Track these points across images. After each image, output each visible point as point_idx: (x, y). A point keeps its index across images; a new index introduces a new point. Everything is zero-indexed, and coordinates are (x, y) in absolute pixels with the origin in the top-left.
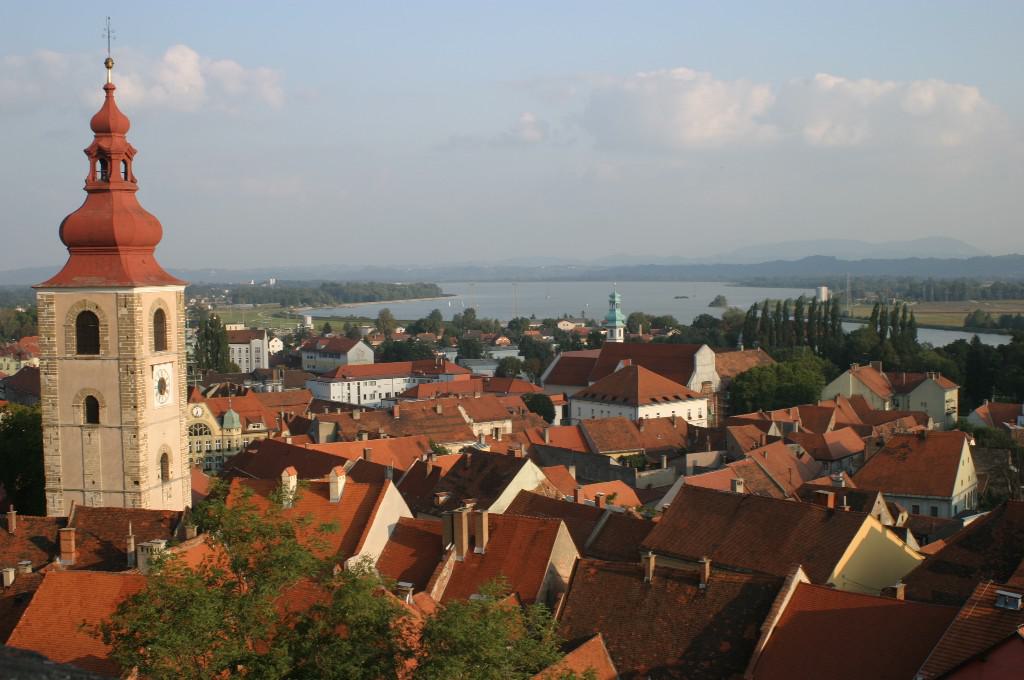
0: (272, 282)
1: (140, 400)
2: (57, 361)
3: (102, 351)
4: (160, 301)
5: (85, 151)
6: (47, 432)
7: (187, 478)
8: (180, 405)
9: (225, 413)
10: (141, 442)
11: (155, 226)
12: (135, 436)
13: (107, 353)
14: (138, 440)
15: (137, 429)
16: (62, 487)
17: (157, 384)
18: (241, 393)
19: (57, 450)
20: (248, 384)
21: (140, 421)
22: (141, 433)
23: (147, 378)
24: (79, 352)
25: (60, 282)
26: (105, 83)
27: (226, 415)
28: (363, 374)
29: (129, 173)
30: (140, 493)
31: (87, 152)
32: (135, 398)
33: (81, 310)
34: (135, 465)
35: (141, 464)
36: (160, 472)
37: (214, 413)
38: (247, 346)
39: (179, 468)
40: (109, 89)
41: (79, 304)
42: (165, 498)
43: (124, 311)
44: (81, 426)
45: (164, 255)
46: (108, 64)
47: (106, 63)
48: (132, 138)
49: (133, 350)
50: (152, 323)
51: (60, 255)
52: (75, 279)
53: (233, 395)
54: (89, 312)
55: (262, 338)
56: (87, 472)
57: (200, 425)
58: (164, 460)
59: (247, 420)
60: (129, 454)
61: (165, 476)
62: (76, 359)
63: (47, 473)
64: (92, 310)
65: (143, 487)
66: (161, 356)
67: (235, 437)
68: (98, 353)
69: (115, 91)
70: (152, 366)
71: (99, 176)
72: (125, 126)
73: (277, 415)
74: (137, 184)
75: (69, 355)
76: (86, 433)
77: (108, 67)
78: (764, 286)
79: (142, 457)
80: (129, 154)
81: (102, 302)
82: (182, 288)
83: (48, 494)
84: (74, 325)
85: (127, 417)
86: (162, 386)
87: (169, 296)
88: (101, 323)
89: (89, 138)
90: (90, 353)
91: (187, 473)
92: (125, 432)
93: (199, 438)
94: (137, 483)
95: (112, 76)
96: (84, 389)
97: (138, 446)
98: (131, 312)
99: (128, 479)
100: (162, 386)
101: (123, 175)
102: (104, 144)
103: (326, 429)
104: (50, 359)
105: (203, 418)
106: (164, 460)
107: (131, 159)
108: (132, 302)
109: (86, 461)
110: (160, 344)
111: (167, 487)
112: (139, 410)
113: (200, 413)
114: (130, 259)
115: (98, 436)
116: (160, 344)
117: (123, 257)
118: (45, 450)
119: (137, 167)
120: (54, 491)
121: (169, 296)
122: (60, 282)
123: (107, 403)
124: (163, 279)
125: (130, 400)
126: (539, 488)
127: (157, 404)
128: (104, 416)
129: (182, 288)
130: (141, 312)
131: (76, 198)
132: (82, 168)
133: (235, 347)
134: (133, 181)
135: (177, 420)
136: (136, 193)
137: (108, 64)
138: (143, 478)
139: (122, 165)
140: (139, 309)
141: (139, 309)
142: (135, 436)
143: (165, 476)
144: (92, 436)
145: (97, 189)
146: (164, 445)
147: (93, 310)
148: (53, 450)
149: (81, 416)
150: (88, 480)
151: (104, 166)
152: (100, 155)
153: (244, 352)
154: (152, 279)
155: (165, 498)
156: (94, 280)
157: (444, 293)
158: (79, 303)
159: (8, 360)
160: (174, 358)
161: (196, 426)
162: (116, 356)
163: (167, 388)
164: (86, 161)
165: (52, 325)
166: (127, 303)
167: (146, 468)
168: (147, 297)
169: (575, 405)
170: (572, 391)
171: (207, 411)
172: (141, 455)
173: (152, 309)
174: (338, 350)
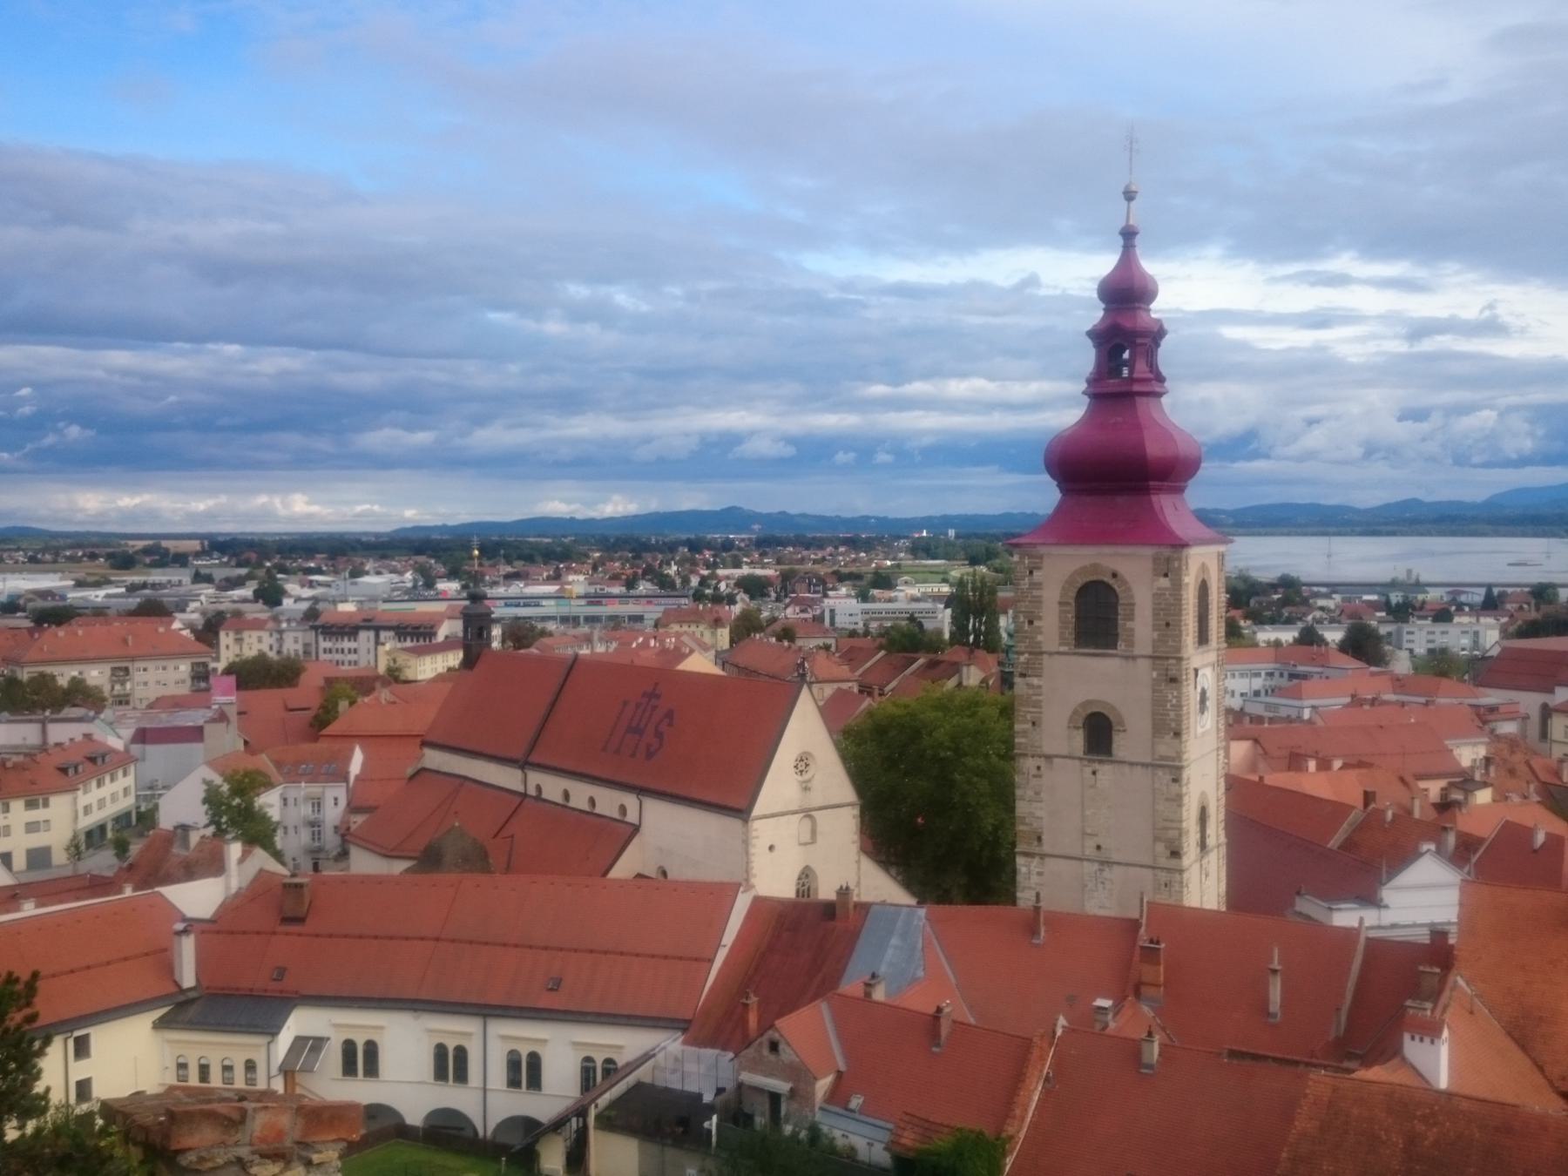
3: (1121, 646)
6: (1029, 764)
10: (1184, 790)
12: (1176, 780)
13: (1131, 644)
14: (1180, 786)
15: (1180, 769)
16: (1046, 848)
21: (1185, 756)
23: (1191, 687)
24: (1078, 645)
26: (1122, 224)
29: (1154, 366)
32: (1179, 720)
34: (1174, 825)
41: (1083, 570)
42: (1204, 876)
43: (1164, 582)
46: (1129, 196)
54: (1101, 583)
62: (1075, 654)
63: (1020, 828)
64: (1106, 579)
68: (1116, 649)
69: (1138, 237)
70: (1196, 671)
74: (1166, 384)
75: (1062, 649)
76: (1088, 770)
83: (1020, 860)
84: (1072, 601)
85: (1163, 749)
88: (1121, 602)
90: (1097, 647)
94: (1176, 854)
95: (1139, 214)
96: (1088, 703)
99: (1160, 847)
104: (1030, 653)
115: (1106, 772)
117: (1154, 498)
118: (1018, 792)
120: (1026, 854)
128: (1122, 745)
135: (1215, 753)
136: (1165, 400)
137: (1129, 196)
144: (1099, 775)
147: (1108, 579)
148: (1030, 793)
159: (701, 628)
165: (1038, 601)
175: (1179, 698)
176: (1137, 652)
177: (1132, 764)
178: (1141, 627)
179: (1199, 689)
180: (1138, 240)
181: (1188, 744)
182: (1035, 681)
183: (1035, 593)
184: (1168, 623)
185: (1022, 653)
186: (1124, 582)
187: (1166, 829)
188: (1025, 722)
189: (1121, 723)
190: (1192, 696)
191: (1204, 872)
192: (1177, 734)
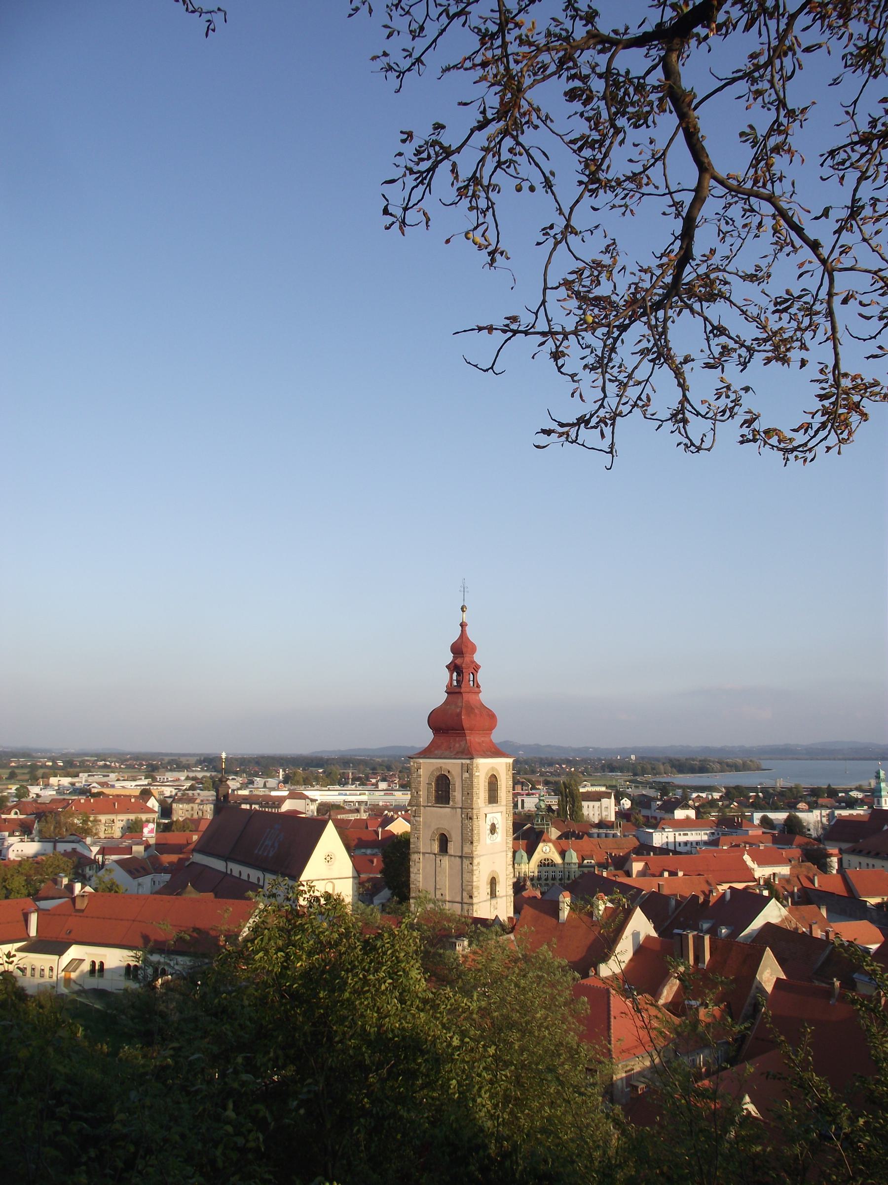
0: (633, 757)
1: (475, 838)
2: (422, 808)
3: (451, 803)
4: (493, 769)
5: (447, 667)
6: (414, 857)
7: (510, 896)
8: (507, 843)
9: (566, 851)
10: (475, 868)
11: (492, 717)
12: (471, 864)
15: (472, 858)
17: (489, 827)
18: (590, 835)
19: (419, 870)
20: (595, 831)
21: (475, 853)
22: (475, 861)
25: (426, 753)
27: (567, 854)
28: (685, 825)
30: (472, 904)
31: (447, 667)
32: (472, 838)
33: (439, 774)
35: (474, 884)
36: (489, 890)
37: (557, 850)
38: (599, 803)
39: (505, 889)
40: (463, 625)
42: (492, 910)
43: (466, 775)
44: (435, 854)
45: (497, 736)
46: (463, 609)
47: (462, 609)
48: (477, 658)
49: (472, 804)
50: (487, 784)
51: (427, 736)
52: (436, 752)
53: (573, 839)
55: (610, 798)
56: (438, 887)
57: (548, 860)
58: (493, 882)
59: (582, 857)
60: (466, 876)
61: (493, 894)
63: (412, 886)
65: (475, 900)
66: (493, 807)
67: (573, 870)
71: (455, 683)
72: (474, 649)
73: (605, 854)
75: (430, 804)
77: (463, 611)
78: (346, 761)
79: (475, 879)
80: (476, 668)
81: (452, 765)
82: (510, 760)
86: (493, 829)
87: (502, 765)
89: (449, 657)
91: (511, 892)
92: (464, 860)
93: (546, 868)
94: (471, 897)
95: (466, 617)
97: (472, 870)
98: (471, 775)
99: (465, 894)
100: (493, 829)
101: (471, 683)
102: (458, 661)
103: (637, 866)
105: (551, 854)
106: (493, 882)
107: (477, 672)
108: (472, 769)
109: (437, 879)
110: (493, 798)
111: (494, 901)
112: (474, 844)
113: (548, 851)
114: (474, 738)
115: (446, 860)
116: (493, 798)
117: (468, 738)
118: (411, 870)
119: (481, 677)
121: (502, 765)
122: (426, 753)
123: (453, 839)
124: (496, 752)
125: (468, 839)
126: (783, 921)
127: (488, 841)
128: (452, 848)
129: (510, 760)
130: (478, 776)
131: (440, 698)
132: (444, 677)
133: (585, 804)
134: (478, 686)
136: (480, 695)
137: (463, 609)
138: (475, 894)
140: (477, 774)
141: (477, 774)
142: (471, 864)
143: (493, 894)
145: (453, 692)
146: (493, 871)
148: (416, 870)
149: (436, 848)
150: (438, 893)
151: (458, 675)
152: (454, 667)
153: (596, 807)
154: (489, 753)
155: (492, 910)
156: (447, 753)
157: (764, 767)
158: (437, 769)
160: (503, 809)
161: (545, 860)
162: (460, 806)
164: (447, 673)
165: (419, 782)
166: (468, 769)
167: (478, 887)
168: (484, 766)
169: (846, 858)
170: (845, 846)
171: (553, 849)
172: (474, 877)
173: (487, 774)
174: (670, 807)
175: (472, 826)
176: (456, 806)
177: (455, 856)
178: (457, 795)
179: (489, 823)
181: (478, 847)
182: (417, 819)
183: (419, 779)
184: (468, 792)
185: (414, 806)
186: (452, 776)
187: (468, 885)
188: (415, 837)
189: (451, 838)
190: (482, 827)
191: (492, 907)
192: (472, 843)
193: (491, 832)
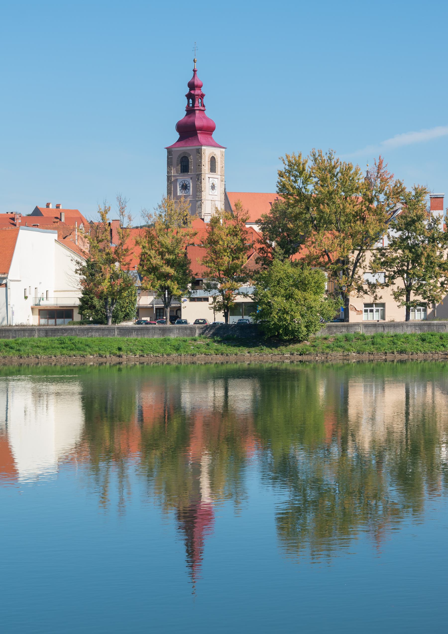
5: (186, 96)
31: (186, 96)
40: (195, 71)
66: (212, 175)
71: (191, 105)
77: (195, 62)
86: (213, 187)
89: (187, 90)
100: (213, 187)
107: (203, 98)
110: (213, 169)
116: (213, 169)
132: (184, 103)
134: (204, 106)
139: (200, 101)
145: (190, 111)
152: (189, 96)
163: (216, 188)
180: (197, 72)
193: (212, 189)
